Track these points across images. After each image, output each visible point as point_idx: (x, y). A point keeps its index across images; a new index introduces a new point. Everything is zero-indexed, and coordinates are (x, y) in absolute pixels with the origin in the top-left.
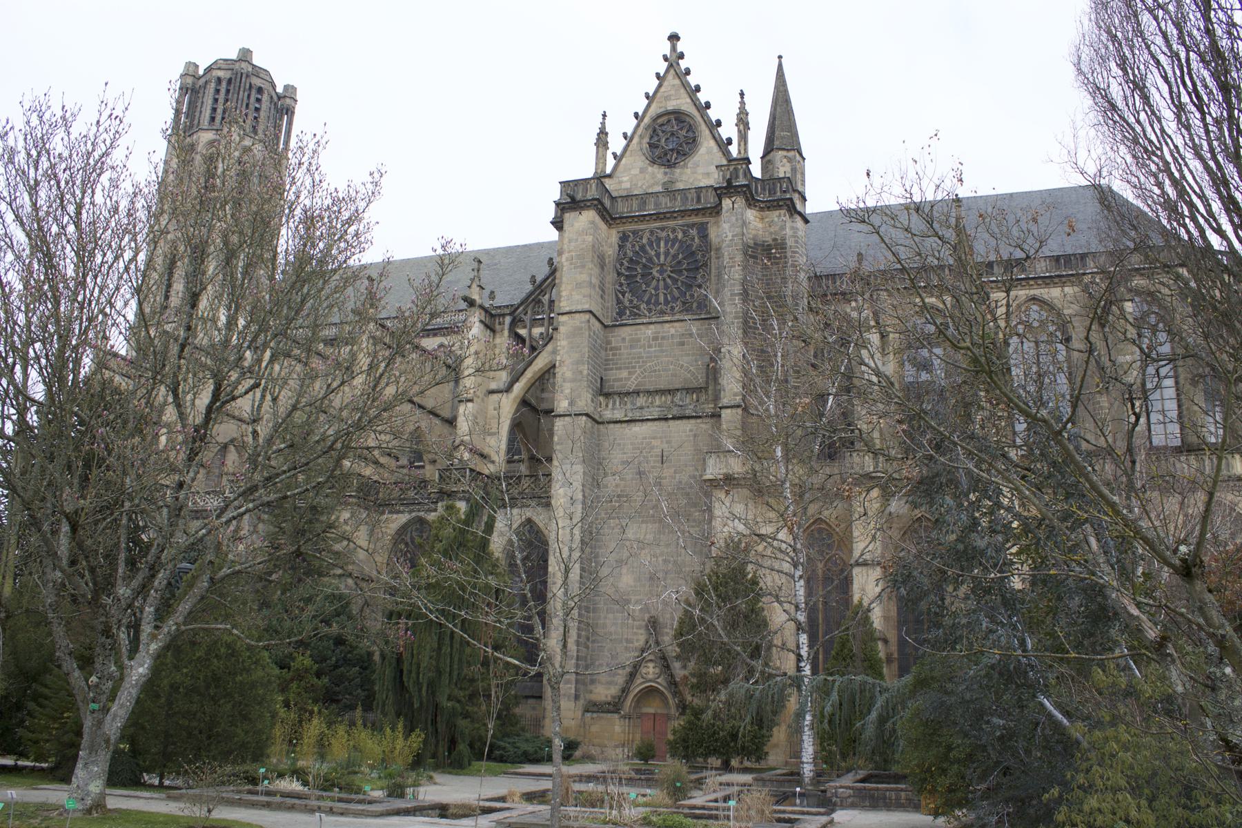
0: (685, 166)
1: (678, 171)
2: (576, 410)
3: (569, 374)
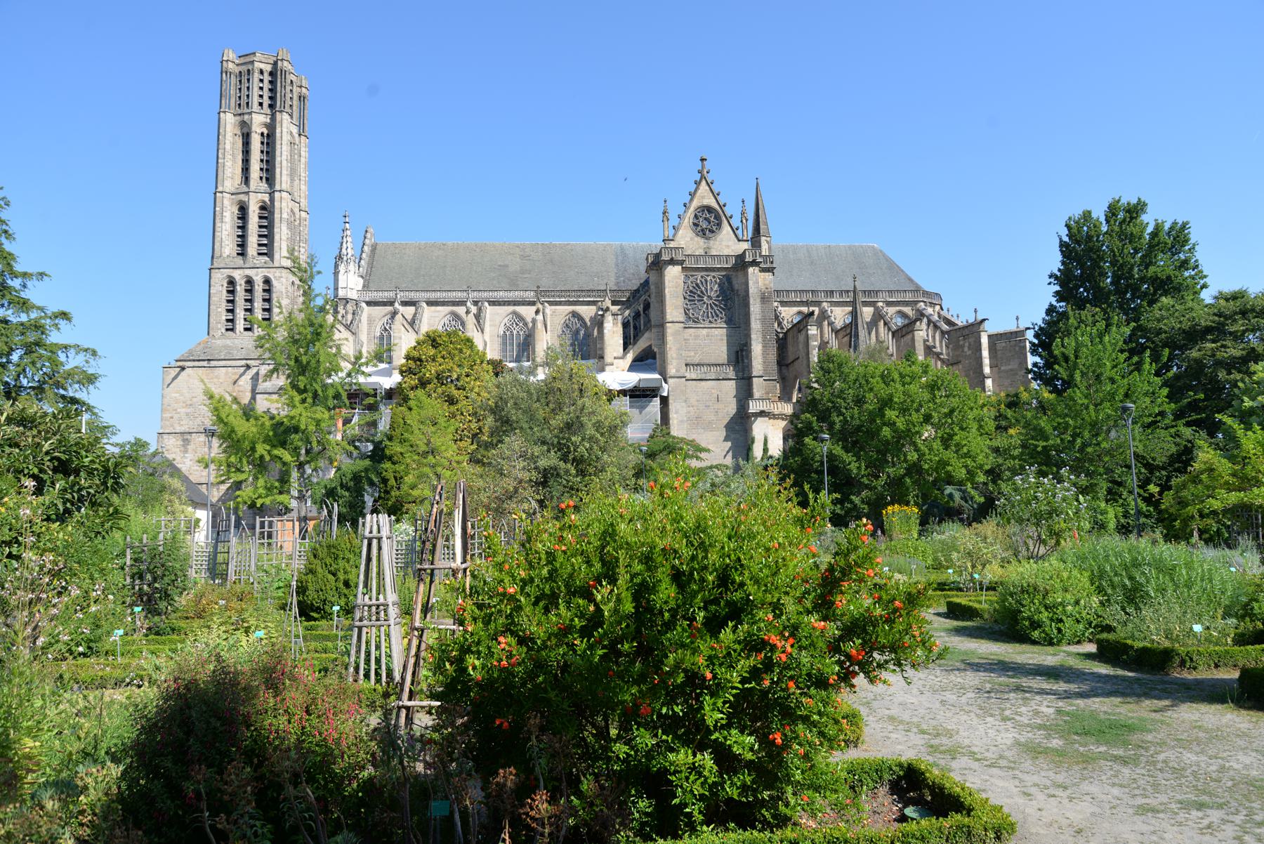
0: (715, 240)
1: (712, 242)
2: (678, 375)
3: (674, 355)
